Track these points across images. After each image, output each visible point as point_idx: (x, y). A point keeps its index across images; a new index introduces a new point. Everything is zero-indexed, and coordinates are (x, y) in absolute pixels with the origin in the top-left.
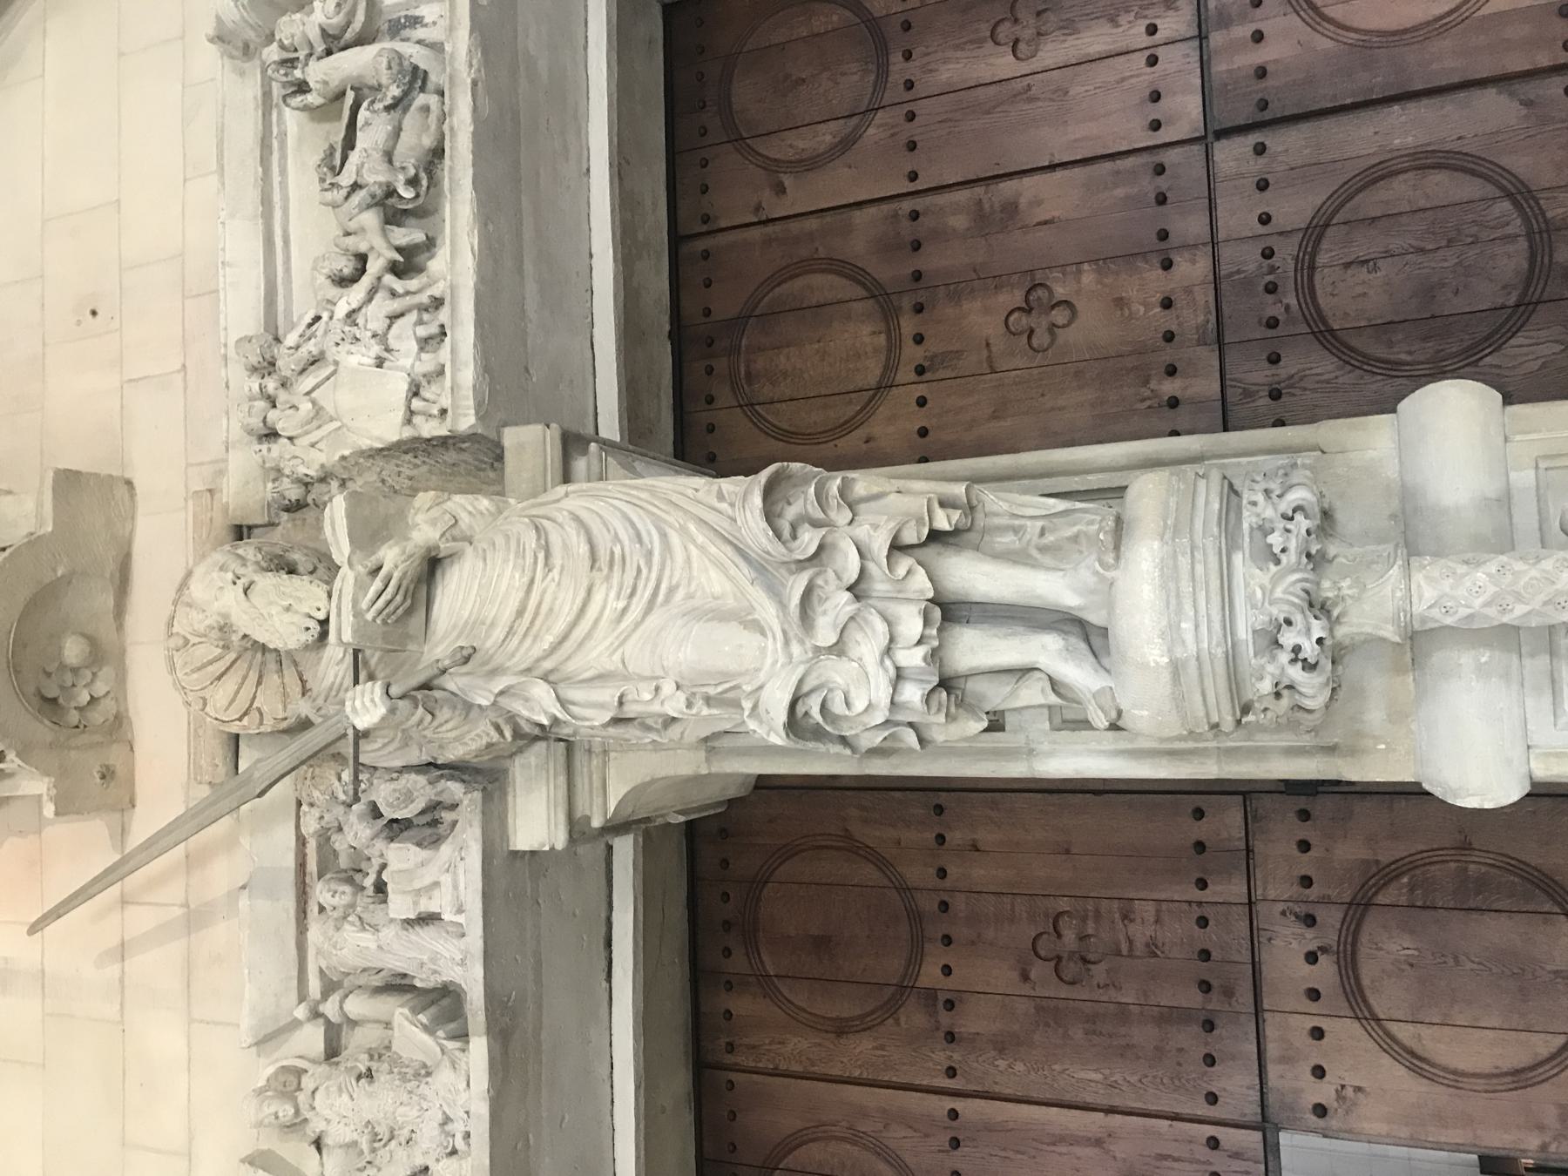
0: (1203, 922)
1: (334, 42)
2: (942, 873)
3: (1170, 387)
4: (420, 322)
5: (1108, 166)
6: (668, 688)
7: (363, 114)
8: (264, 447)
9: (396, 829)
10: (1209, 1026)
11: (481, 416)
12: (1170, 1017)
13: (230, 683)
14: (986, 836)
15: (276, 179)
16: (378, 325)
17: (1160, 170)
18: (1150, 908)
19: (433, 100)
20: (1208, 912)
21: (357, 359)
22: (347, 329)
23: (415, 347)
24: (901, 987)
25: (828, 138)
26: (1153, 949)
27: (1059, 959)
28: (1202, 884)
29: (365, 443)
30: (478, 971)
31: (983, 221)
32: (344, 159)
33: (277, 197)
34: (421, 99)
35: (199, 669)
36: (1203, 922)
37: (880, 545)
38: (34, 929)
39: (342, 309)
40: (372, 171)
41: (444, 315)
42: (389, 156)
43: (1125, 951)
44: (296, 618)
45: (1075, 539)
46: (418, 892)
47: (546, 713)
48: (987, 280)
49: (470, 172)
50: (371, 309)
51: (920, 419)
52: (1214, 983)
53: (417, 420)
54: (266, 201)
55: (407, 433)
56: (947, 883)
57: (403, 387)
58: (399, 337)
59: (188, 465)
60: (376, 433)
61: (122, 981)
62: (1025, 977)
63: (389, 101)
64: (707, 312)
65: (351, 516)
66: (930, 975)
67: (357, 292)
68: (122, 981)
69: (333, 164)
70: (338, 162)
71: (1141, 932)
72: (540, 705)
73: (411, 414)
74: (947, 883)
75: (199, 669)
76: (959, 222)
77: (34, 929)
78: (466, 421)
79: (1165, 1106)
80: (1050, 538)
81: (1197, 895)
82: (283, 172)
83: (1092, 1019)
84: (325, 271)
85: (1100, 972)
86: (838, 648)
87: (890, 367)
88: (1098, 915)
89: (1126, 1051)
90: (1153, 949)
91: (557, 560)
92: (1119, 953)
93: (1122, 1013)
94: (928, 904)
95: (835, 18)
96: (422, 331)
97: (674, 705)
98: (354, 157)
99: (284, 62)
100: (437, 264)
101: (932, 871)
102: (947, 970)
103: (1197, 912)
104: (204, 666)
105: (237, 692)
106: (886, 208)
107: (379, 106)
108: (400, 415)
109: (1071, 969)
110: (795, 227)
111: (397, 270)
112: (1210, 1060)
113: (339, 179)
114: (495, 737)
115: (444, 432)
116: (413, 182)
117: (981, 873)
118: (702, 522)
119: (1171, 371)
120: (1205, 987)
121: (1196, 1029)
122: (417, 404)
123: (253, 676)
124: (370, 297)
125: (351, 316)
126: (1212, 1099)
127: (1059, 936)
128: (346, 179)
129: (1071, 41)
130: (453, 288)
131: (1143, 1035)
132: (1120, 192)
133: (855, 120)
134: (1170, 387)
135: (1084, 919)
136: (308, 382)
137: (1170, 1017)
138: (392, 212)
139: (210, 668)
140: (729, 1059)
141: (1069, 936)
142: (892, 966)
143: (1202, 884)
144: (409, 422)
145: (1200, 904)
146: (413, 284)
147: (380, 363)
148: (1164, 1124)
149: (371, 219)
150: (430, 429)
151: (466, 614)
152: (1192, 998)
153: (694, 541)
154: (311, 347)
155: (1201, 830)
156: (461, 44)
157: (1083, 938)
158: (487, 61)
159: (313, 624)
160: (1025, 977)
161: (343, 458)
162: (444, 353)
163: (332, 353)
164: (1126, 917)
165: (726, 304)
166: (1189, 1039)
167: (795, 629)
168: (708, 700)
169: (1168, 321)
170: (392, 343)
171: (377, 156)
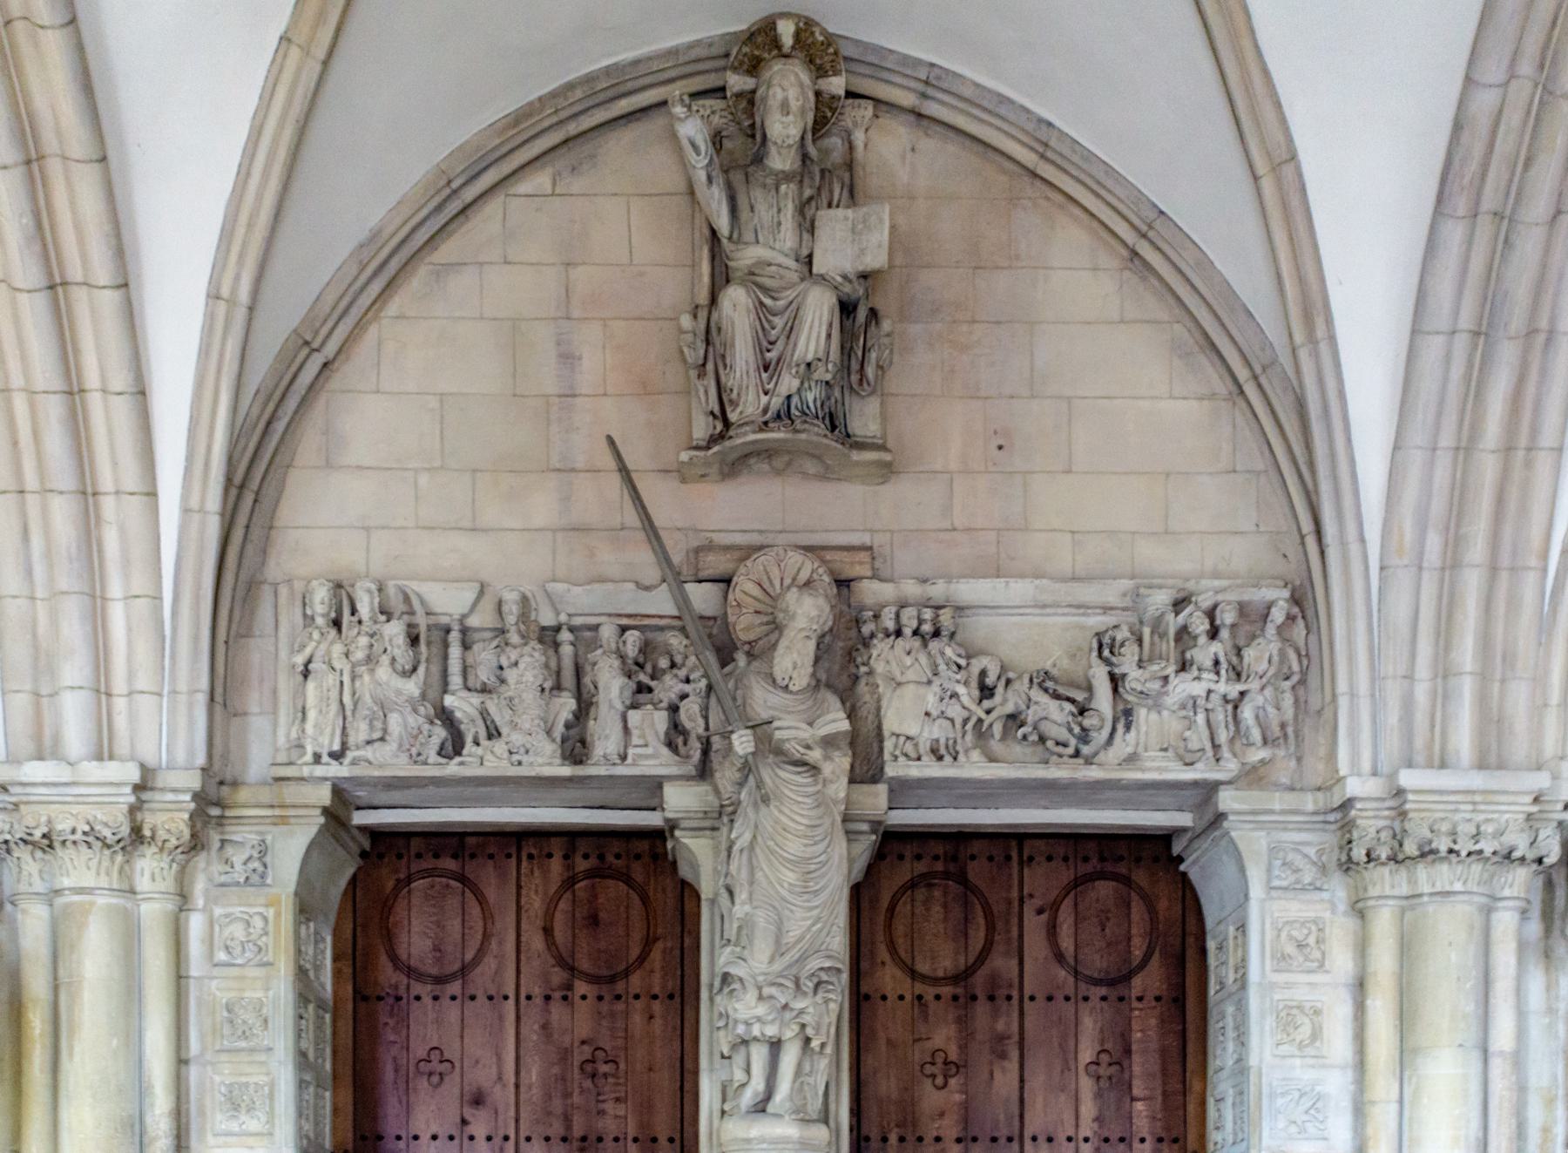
0: (616, 1139)
1: (1116, 681)
2: (637, 997)
3: (893, 1138)
4: (947, 739)
5: (1017, 1112)
6: (747, 908)
7: (1068, 707)
8: (893, 616)
9: (674, 709)
10: (564, 1139)
11: (892, 778)
12: (567, 1119)
13: (756, 592)
14: (658, 1023)
15: (1060, 611)
16: (950, 713)
17: (1010, 1139)
18: (622, 1113)
19: (1071, 750)
20: (621, 1143)
21: (931, 700)
22: (949, 693)
23: (935, 736)
24: (572, 969)
25: (1065, 945)
26: (602, 1113)
27: (594, 1062)
28: (635, 1140)
29: (884, 703)
30: (602, 771)
31: (1001, 1038)
32: (1046, 690)
33: (1048, 610)
34: (1073, 742)
35: (765, 570)
36: (616, 1139)
37: (806, 1019)
38: (611, 441)
39: (961, 690)
40: (1035, 712)
41: (948, 759)
42: (1046, 718)
43: (601, 1098)
44: (790, 669)
45: (805, 1098)
46: (642, 729)
47: (737, 838)
48: (966, 1038)
49: (1025, 776)
50: (958, 708)
51: (892, 996)
52: (586, 1144)
53: (894, 738)
54: (1044, 606)
55: (886, 733)
56: (631, 1000)
57: (912, 732)
58: (940, 726)
59: (892, 532)
60: (889, 714)
61: (573, 470)
62: (583, 1042)
63: (1073, 726)
64: (973, 857)
65: (838, 733)
66: (581, 987)
67: (967, 694)
68: (573, 470)
69: (1044, 681)
70: (1049, 684)
71: (609, 1107)
72: (742, 834)
73: (898, 736)
74: (631, 1000)
75: (765, 570)
76: (1000, 1026)
77: (611, 441)
78: (891, 771)
79: (523, 1115)
80: (806, 1088)
81: (630, 1138)
82: (1064, 615)
83: (564, 1079)
84: (989, 667)
85: (588, 1083)
86: (761, 998)
87: (924, 978)
88: (617, 1084)
89: (548, 1097)
90: (602, 1113)
91: (810, 849)
92: (599, 1094)
93: (567, 1095)
94: (620, 987)
95: (1137, 953)
96: (942, 741)
97: (740, 910)
98: (1044, 699)
99: (1114, 640)
100: (976, 755)
101: (638, 991)
102: (584, 997)
103: (622, 1137)
104: (767, 573)
105: (751, 596)
106: (1016, 981)
107: (1070, 718)
108: (898, 732)
109: (589, 1068)
110: (1015, 920)
111: (980, 721)
112: (547, 1139)
113: (1035, 687)
114: (727, 796)
115: (887, 756)
116: (1025, 737)
117: (637, 1019)
118: (821, 930)
119: (902, 1139)
120: (584, 1139)
121: (562, 1132)
122: (902, 739)
123: (760, 607)
124: (964, 708)
125: (954, 695)
126: (528, 1139)
127: (606, 1062)
128: (1037, 694)
129: (1090, 1095)
130: (962, 766)
131: (557, 1105)
132: (1002, 1117)
133: (1073, 963)
134: (893, 1138)
135: (613, 1076)
136: (923, 659)
137: (567, 1119)
138: (1014, 719)
139: (765, 578)
140: (524, 858)
141: (604, 1068)
142: (584, 964)
143: (635, 1140)
144: (893, 734)
145: (625, 1139)
146: (969, 737)
147: (927, 714)
148: (512, 1113)
149: (1009, 708)
150: (889, 745)
151: (787, 792)
152: (578, 1131)
153: (813, 925)
154: (942, 667)
155: (663, 1141)
156: (1094, 773)
157: (605, 1075)
158: (1088, 783)
159: (785, 683)
160: (583, 1042)
161: (878, 686)
162: (928, 759)
163: (937, 682)
164: (617, 1100)
165: (977, 872)
166: (557, 1129)
167: (770, 978)
168: (740, 928)
169: (929, 1139)
170: (939, 721)
171: (1044, 714)
